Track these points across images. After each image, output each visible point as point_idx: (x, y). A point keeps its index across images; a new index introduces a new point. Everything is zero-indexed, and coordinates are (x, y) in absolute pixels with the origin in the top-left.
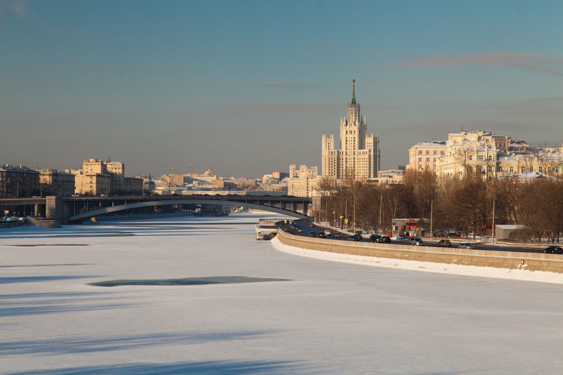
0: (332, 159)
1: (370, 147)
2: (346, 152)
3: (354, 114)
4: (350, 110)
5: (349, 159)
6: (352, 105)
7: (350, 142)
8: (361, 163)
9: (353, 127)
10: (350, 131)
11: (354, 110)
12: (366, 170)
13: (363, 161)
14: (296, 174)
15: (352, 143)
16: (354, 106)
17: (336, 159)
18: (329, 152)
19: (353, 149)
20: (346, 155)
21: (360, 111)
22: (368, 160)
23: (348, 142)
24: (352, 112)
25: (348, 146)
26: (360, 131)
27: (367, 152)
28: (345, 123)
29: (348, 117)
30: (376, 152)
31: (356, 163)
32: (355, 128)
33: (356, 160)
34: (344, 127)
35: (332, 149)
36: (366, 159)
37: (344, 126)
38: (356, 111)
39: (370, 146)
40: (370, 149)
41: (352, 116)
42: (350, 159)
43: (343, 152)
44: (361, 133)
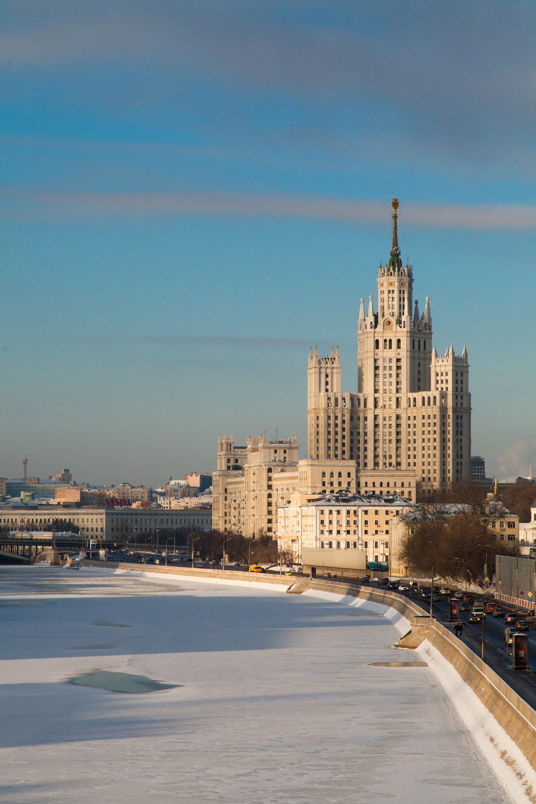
0: (336, 418)
1: (444, 386)
2: (375, 399)
3: (396, 295)
4: (386, 284)
5: (384, 419)
6: (391, 271)
8: (419, 429)
9: (394, 329)
10: (386, 341)
11: (396, 284)
12: (432, 448)
13: (424, 424)
14: (237, 461)
15: (390, 375)
16: (396, 273)
17: (347, 418)
18: (329, 399)
19: (394, 391)
20: (376, 407)
21: (414, 285)
22: (437, 421)
23: (381, 371)
24: (391, 289)
25: (381, 384)
26: (413, 341)
27: (435, 397)
28: (371, 319)
29: (380, 304)
31: (404, 429)
32: (401, 332)
33: (404, 422)
34: (369, 329)
35: (335, 390)
36: (432, 417)
37: (369, 326)
38: (401, 284)
39: (442, 381)
40: (444, 390)
41: (391, 299)
42: (387, 419)
43: (365, 400)
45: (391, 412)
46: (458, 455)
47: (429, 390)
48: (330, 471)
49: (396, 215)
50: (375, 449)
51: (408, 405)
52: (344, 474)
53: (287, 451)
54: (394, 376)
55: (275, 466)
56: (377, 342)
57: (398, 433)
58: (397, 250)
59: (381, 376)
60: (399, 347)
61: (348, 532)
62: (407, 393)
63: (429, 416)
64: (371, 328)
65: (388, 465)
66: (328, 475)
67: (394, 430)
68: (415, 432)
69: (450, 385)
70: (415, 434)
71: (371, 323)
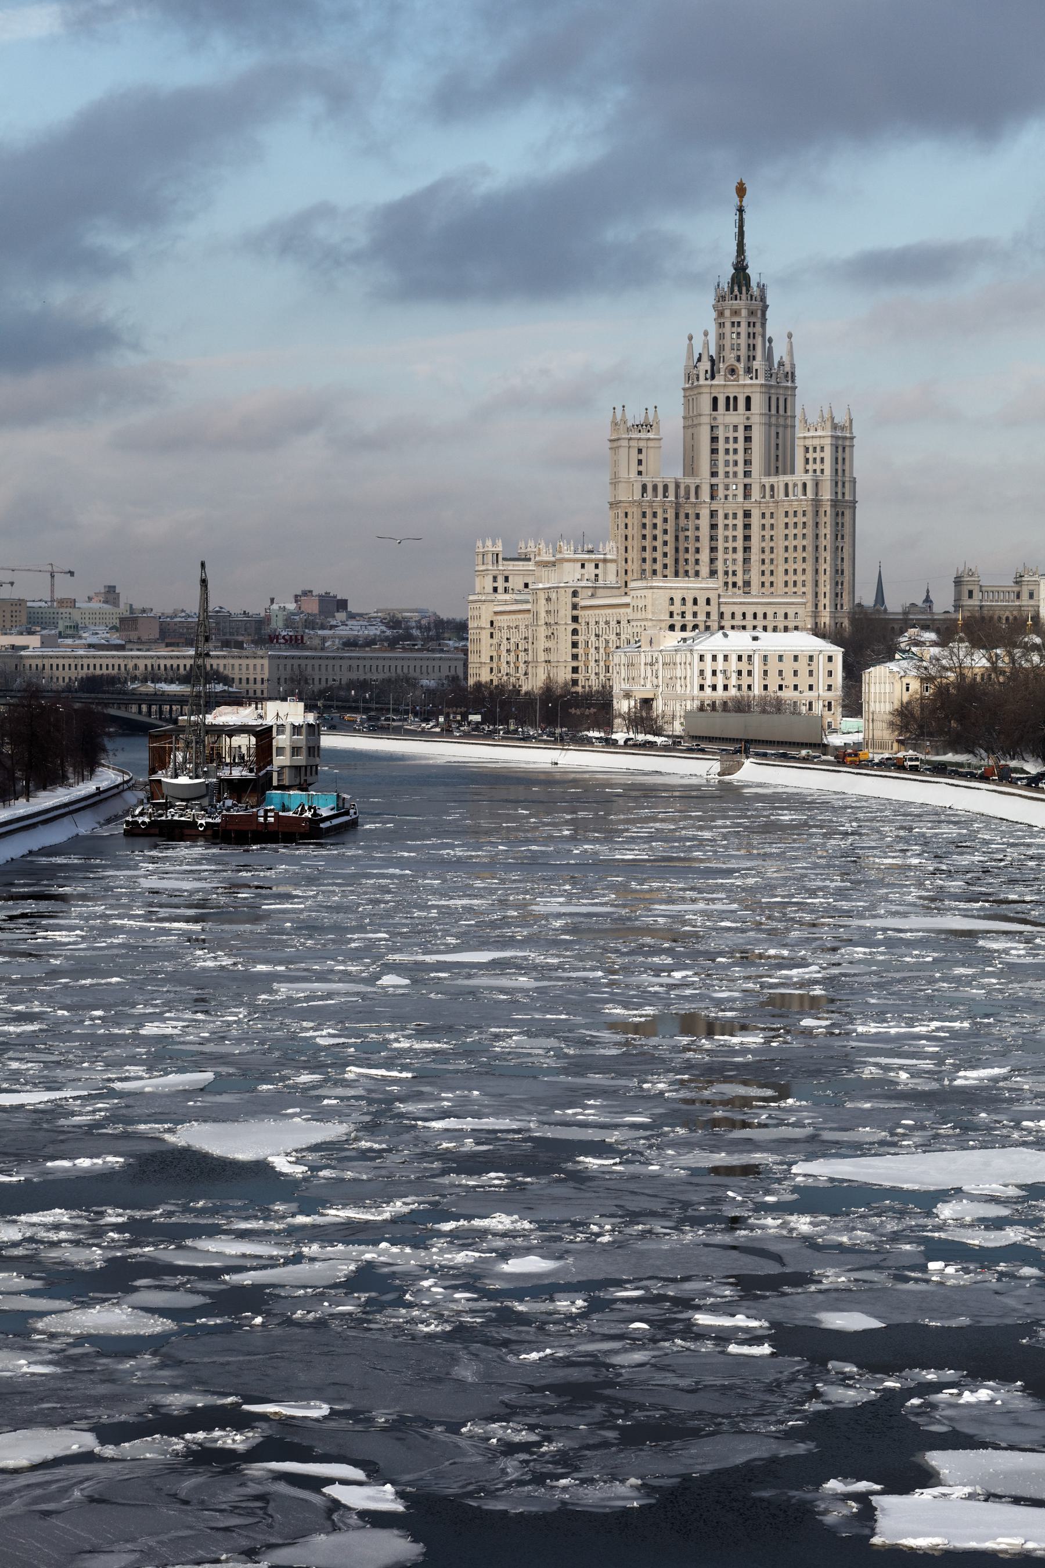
0: (655, 515)
3: (743, 329)
5: (726, 516)
8: (780, 531)
10: (728, 398)
17: (670, 515)
19: (741, 474)
20: (712, 498)
21: (769, 314)
22: (809, 519)
23: (721, 446)
24: (736, 319)
27: (805, 485)
30: (840, 484)
31: (755, 532)
33: (755, 521)
36: (800, 514)
39: (815, 459)
41: (734, 336)
44: (773, 411)
45: (736, 503)
46: (837, 571)
47: (793, 472)
48: (680, 597)
49: (741, 206)
50: (712, 561)
52: (702, 601)
53: (601, 565)
54: (741, 451)
55: (583, 587)
56: (715, 400)
57: (747, 538)
58: (743, 260)
59: (721, 452)
60: (748, 408)
61: (714, 688)
63: (795, 512)
64: (706, 379)
65: (730, 585)
66: (678, 601)
67: (740, 533)
68: (772, 536)
69: (827, 466)
70: (772, 540)
71: (707, 371)
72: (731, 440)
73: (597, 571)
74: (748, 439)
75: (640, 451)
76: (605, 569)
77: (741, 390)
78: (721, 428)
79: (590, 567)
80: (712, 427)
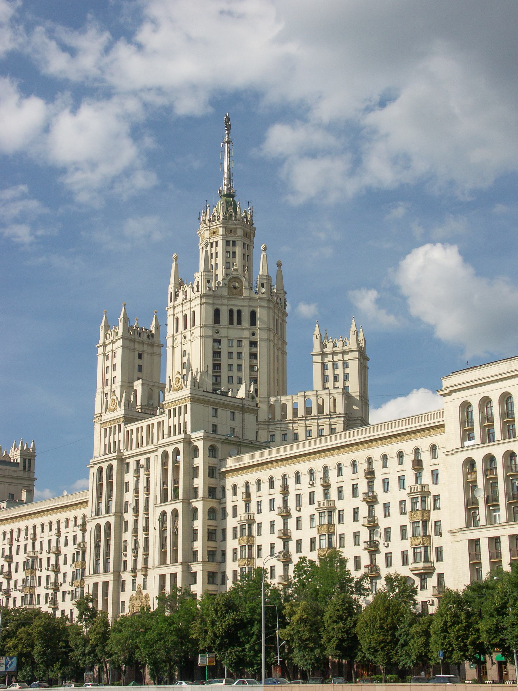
3: (238, 250)
7: (235, 361)
9: (245, 293)
10: (231, 312)
23: (224, 360)
24: (231, 238)
51: (270, 417)
53: (238, 415)
56: (217, 313)
60: (253, 322)
62: (269, 398)
72: (235, 355)
73: (233, 424)
74: (253, 356)
75: (140, 356)
76: (243, 421)
77: (246, 303)
78: (224, 342)
79: (224, 414)
80: (215, 341)
